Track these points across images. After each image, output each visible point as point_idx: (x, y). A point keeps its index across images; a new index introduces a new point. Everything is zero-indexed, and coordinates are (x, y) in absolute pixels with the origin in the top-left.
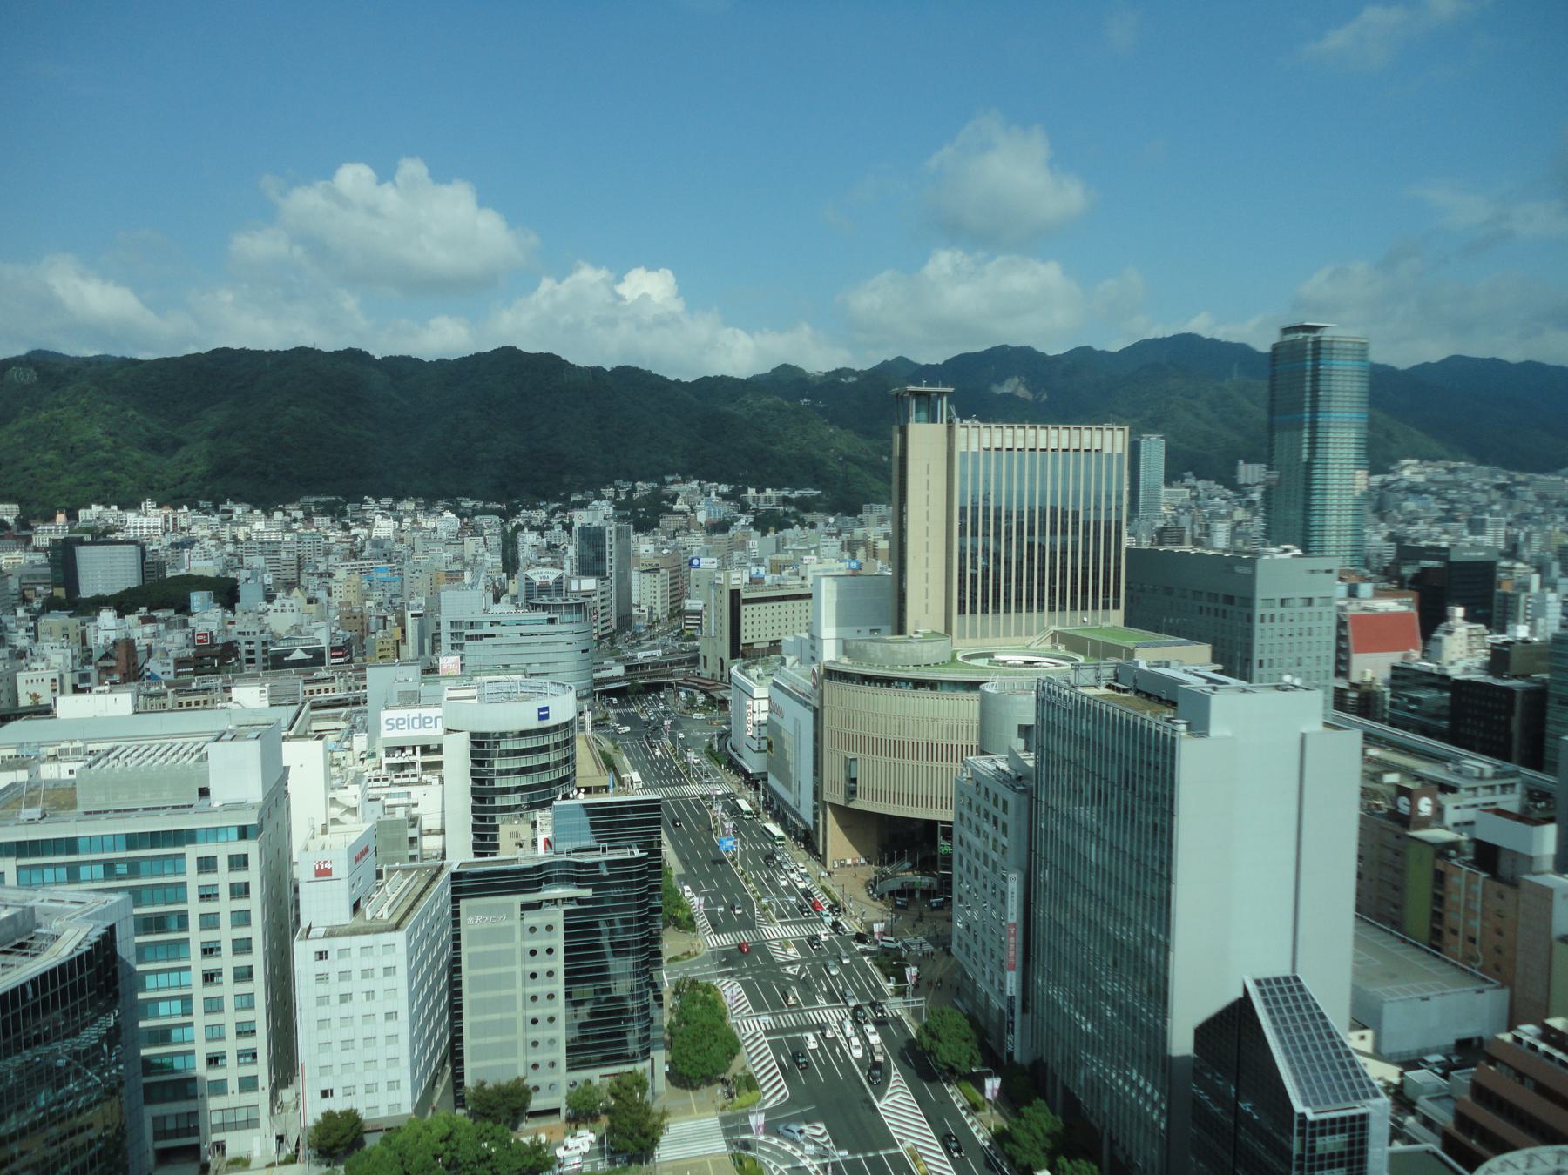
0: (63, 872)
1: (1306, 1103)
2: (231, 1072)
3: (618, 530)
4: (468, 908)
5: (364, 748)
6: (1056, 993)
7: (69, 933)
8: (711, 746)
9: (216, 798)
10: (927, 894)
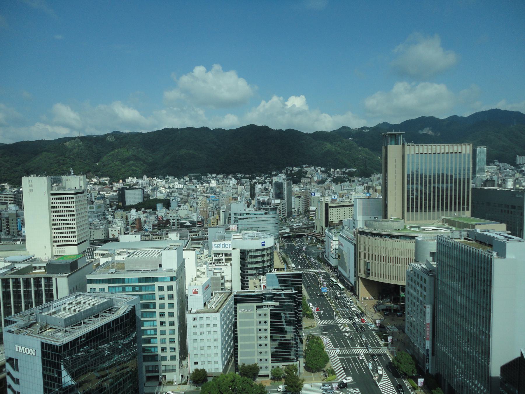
0: (121, 288)
2: (168, 354)
3: (288, 183)
4: (240, 307)
5: (207, 253)
6: (445, 350)
7: (122, 307)
8: (318, 256)
9: (164, 268)
10: (396, 311)
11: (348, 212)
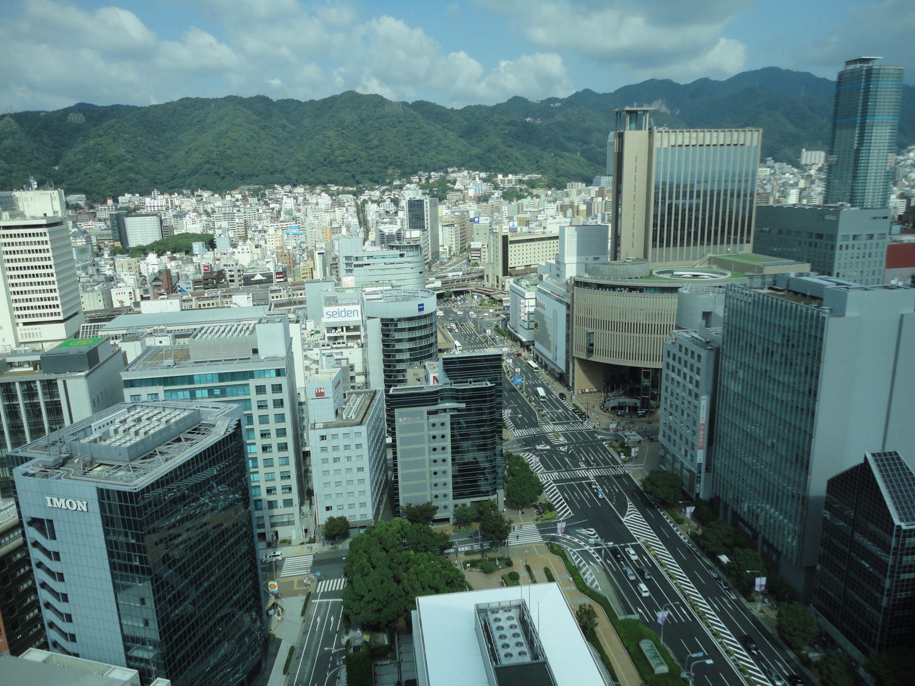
0: (187, 394)
1: (901, 520)
3: (431, 201)
4: (400, 413)
8: (497, 326)
9: (262, 354)
10: (634, 409)
11: (541, 250)
